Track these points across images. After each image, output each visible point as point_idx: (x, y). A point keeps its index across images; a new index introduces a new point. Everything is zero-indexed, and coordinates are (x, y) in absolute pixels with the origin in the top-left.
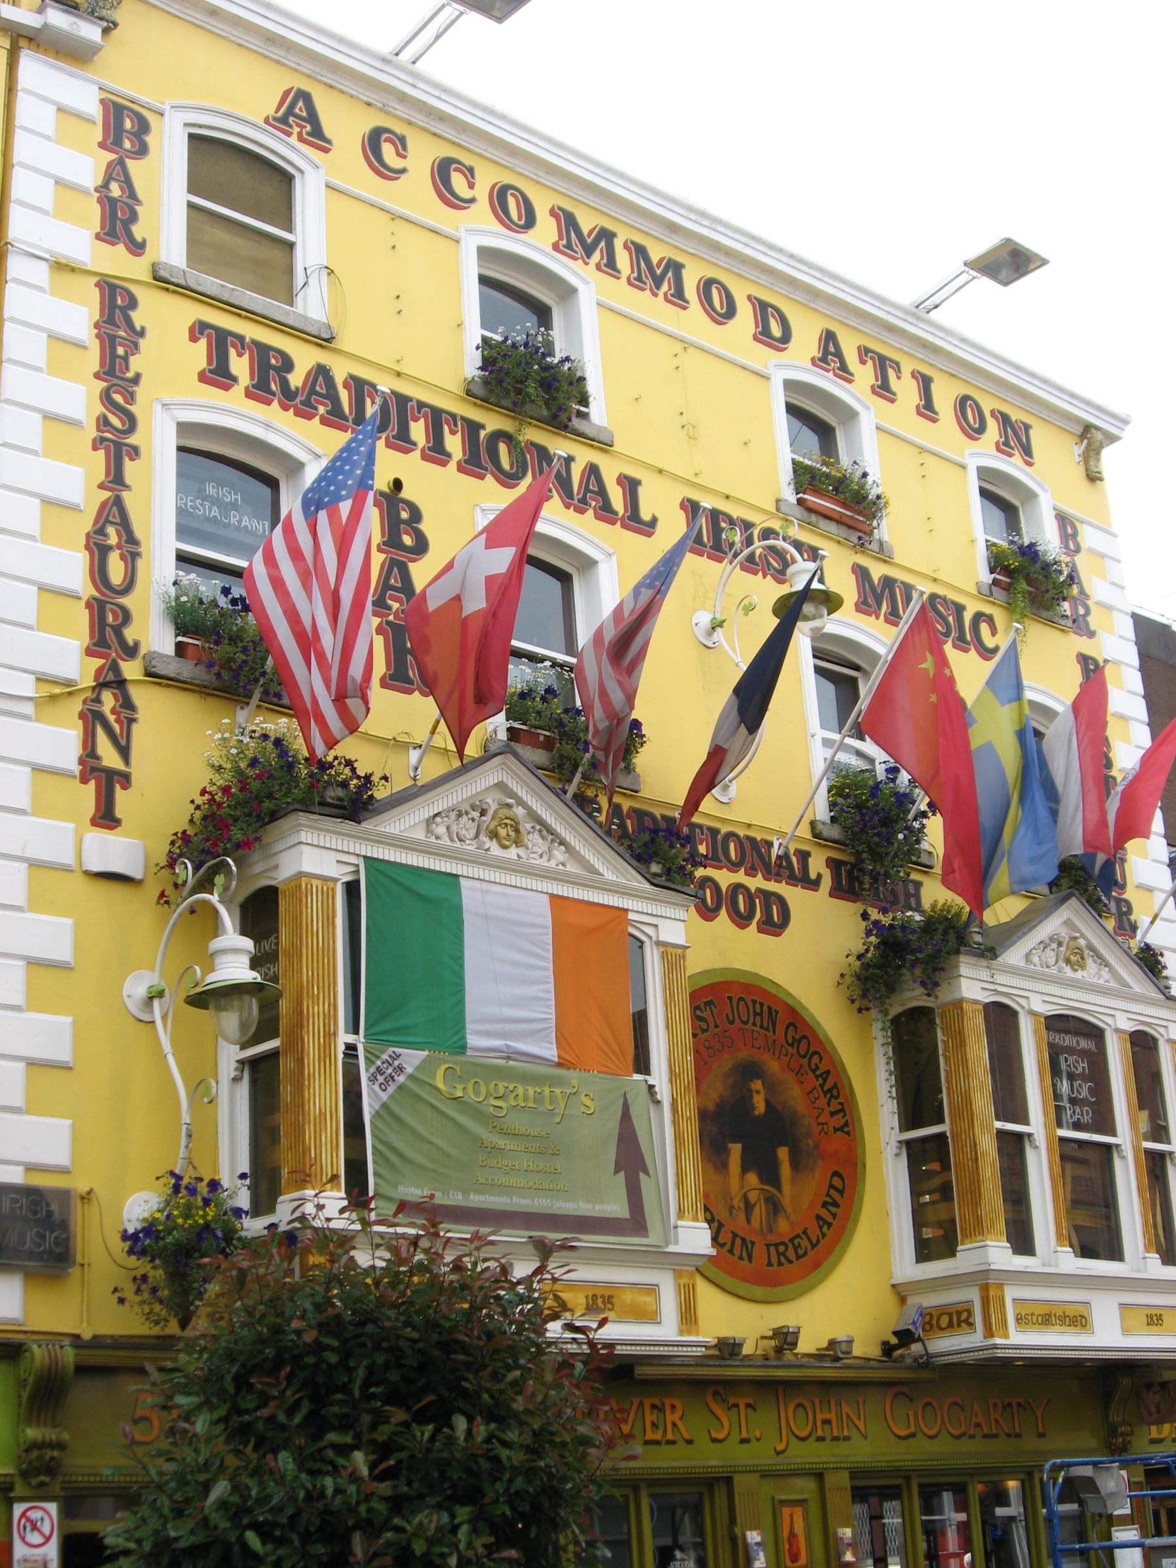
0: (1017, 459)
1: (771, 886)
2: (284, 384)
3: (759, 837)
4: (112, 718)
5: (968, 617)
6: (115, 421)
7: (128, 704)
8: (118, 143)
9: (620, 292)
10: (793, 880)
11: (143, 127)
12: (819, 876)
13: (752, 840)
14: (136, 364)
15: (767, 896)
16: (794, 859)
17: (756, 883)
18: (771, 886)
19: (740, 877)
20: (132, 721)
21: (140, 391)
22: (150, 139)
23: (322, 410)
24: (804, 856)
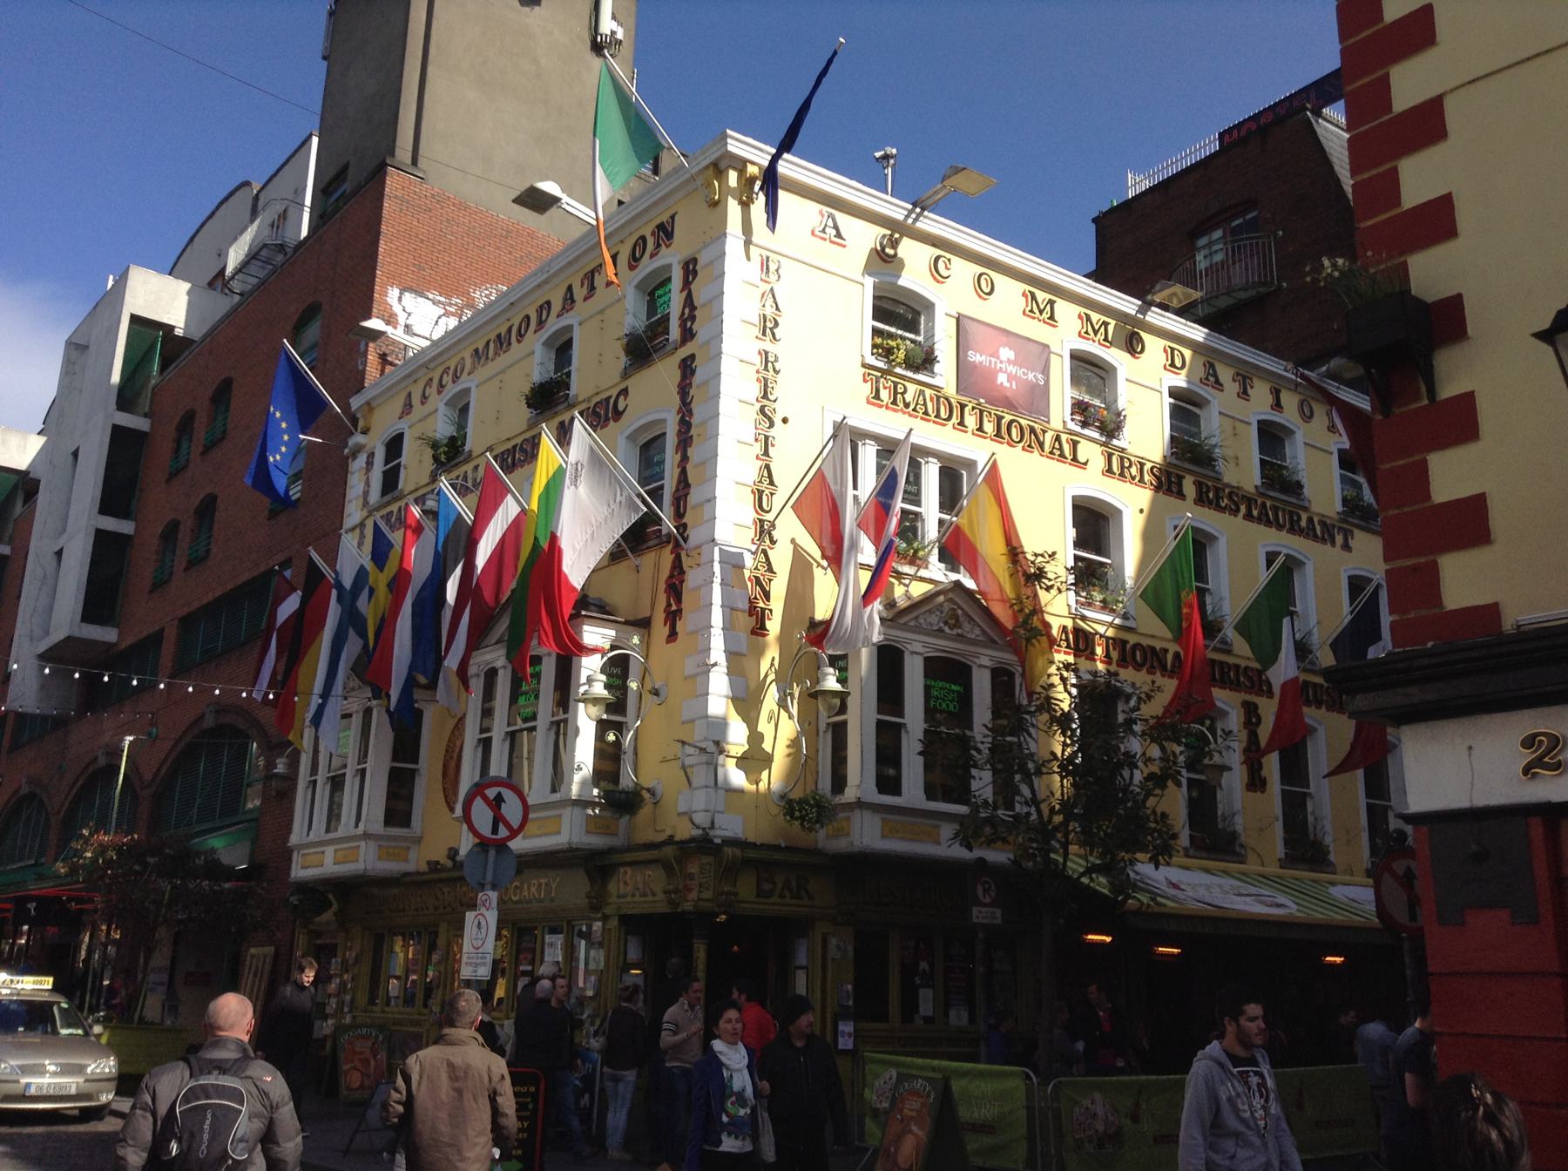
5: (612, 401)
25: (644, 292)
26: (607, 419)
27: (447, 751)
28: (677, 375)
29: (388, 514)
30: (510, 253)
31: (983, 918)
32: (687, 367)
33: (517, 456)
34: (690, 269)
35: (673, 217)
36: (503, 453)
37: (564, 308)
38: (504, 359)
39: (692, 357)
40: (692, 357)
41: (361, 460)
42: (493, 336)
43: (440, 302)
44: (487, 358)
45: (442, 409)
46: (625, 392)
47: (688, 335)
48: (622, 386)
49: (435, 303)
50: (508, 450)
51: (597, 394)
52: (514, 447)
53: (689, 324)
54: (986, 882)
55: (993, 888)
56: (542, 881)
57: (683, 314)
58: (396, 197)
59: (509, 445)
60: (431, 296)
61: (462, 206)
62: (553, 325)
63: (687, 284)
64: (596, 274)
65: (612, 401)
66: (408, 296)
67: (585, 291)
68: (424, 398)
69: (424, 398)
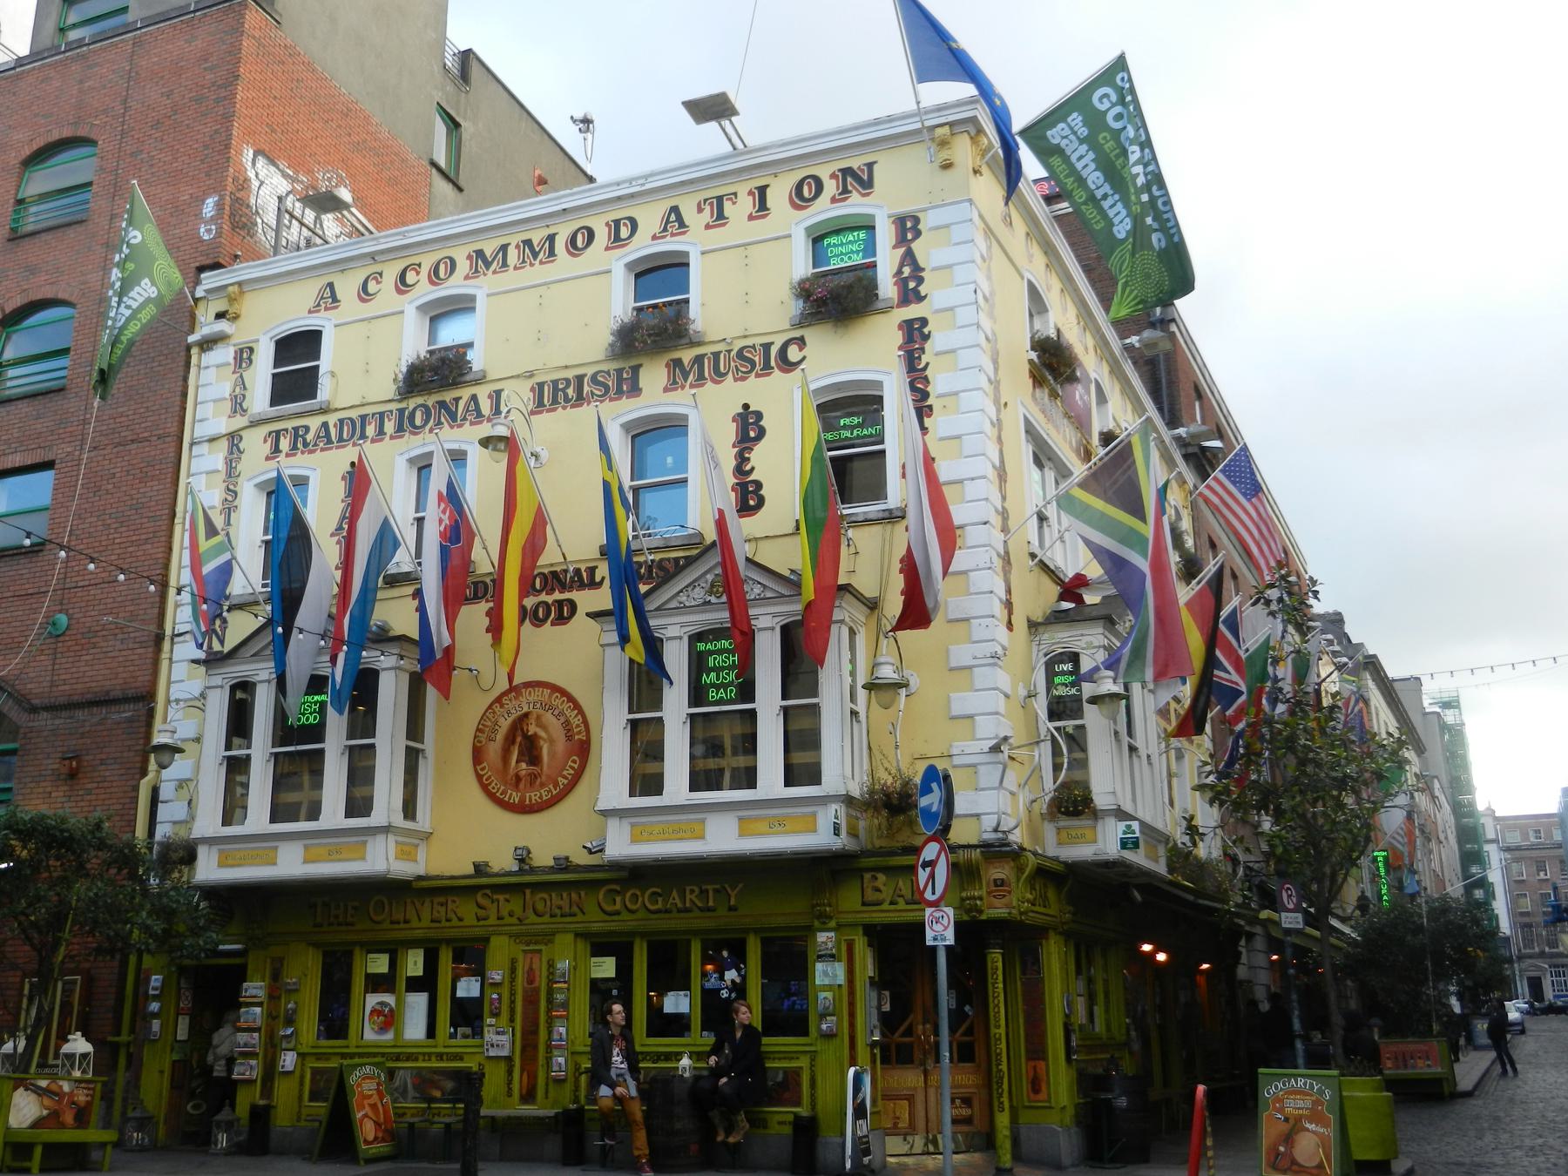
0: (855, 197)
1: (567, 595)
2: (305, 440)
3: (558, 569)
4: (218, 630)
5: (774, 350)
6: (230, 498)
7: (225, 621)
8: (240, 367)
9: (510, 278)
10: (582, 586)
11: (251, 350)
12: (603, 578)
13: (554, 574)
14: (239, 468)
15: (560, 603)
16: (585, 575)
17: (557, 596)
18: (567, 595)
19: (544, 597)
20: (225, 628)
21: (240, 480)
22: (253, 357)
23: (321, 445)
24: (592, 570)
25: (809, 236)
26: (767, 366)
27: (478, 730)
28: (898, 338)
29: (296, 429)
30: (350, 135)
31: (1290, 923)
32: (915, 334)
33: (586, 389)
34: (907, 228)
35: (870, 166)
36: (555, 382)
37: (665, 230)
38: (537, 272)
39: (924, 322)
40: (924, 322)
41: (223, 354)
42: (515, 240)
43: (290, 177)
44: (505, 264)
45: (411, 312)
46: (801, 342)
47: (909, 295)
48: (797, 334)
49: (285, 175)
50: (568, 381)
51: (745, 337)
52: (580, 379)
53: (912, 285)
54: (1289, 889)
55: (1294, 894)
56: (710, 887)
57: (899, 272)
58: (254, 37)
59: (570, 374)
60: (281, 166)
61: (309, 65)
62: (643, 246)
63: (902, 240)
64: (727, 205)
65: (774, 350)
66: (261, 162)
67: (706, 216)
68: (365, 294)
69: (365, 294)
